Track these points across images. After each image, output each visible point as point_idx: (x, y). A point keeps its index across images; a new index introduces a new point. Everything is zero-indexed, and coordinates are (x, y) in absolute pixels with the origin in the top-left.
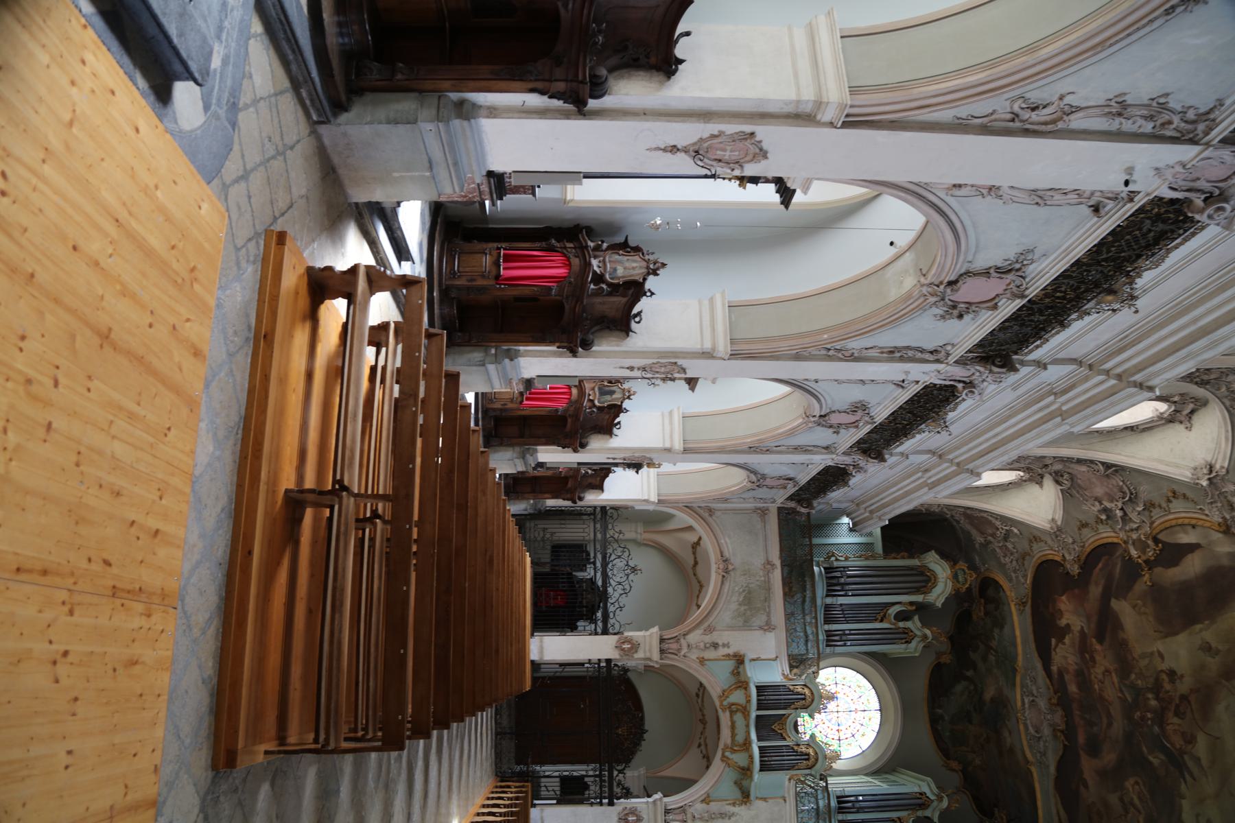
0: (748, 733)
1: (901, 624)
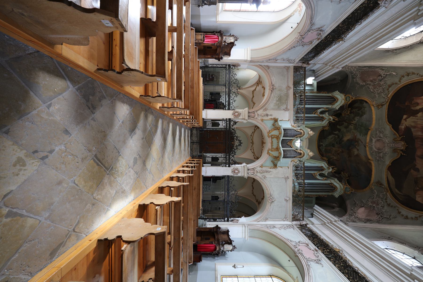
0: (278, 145)
1: (321, 115)
